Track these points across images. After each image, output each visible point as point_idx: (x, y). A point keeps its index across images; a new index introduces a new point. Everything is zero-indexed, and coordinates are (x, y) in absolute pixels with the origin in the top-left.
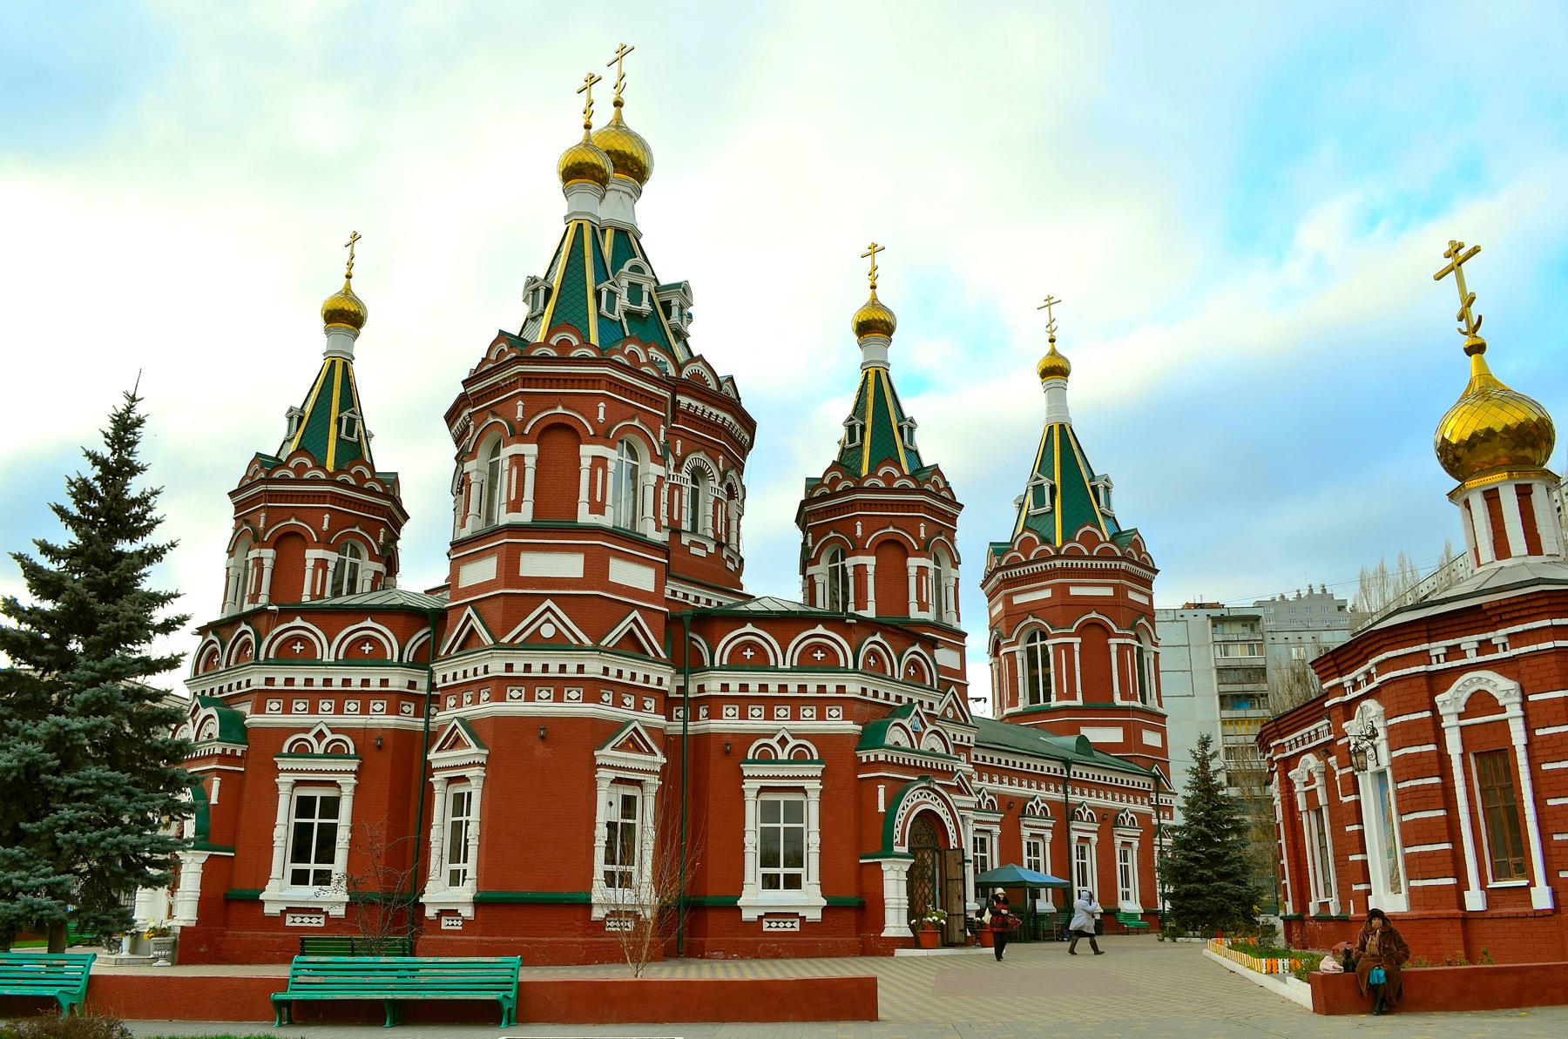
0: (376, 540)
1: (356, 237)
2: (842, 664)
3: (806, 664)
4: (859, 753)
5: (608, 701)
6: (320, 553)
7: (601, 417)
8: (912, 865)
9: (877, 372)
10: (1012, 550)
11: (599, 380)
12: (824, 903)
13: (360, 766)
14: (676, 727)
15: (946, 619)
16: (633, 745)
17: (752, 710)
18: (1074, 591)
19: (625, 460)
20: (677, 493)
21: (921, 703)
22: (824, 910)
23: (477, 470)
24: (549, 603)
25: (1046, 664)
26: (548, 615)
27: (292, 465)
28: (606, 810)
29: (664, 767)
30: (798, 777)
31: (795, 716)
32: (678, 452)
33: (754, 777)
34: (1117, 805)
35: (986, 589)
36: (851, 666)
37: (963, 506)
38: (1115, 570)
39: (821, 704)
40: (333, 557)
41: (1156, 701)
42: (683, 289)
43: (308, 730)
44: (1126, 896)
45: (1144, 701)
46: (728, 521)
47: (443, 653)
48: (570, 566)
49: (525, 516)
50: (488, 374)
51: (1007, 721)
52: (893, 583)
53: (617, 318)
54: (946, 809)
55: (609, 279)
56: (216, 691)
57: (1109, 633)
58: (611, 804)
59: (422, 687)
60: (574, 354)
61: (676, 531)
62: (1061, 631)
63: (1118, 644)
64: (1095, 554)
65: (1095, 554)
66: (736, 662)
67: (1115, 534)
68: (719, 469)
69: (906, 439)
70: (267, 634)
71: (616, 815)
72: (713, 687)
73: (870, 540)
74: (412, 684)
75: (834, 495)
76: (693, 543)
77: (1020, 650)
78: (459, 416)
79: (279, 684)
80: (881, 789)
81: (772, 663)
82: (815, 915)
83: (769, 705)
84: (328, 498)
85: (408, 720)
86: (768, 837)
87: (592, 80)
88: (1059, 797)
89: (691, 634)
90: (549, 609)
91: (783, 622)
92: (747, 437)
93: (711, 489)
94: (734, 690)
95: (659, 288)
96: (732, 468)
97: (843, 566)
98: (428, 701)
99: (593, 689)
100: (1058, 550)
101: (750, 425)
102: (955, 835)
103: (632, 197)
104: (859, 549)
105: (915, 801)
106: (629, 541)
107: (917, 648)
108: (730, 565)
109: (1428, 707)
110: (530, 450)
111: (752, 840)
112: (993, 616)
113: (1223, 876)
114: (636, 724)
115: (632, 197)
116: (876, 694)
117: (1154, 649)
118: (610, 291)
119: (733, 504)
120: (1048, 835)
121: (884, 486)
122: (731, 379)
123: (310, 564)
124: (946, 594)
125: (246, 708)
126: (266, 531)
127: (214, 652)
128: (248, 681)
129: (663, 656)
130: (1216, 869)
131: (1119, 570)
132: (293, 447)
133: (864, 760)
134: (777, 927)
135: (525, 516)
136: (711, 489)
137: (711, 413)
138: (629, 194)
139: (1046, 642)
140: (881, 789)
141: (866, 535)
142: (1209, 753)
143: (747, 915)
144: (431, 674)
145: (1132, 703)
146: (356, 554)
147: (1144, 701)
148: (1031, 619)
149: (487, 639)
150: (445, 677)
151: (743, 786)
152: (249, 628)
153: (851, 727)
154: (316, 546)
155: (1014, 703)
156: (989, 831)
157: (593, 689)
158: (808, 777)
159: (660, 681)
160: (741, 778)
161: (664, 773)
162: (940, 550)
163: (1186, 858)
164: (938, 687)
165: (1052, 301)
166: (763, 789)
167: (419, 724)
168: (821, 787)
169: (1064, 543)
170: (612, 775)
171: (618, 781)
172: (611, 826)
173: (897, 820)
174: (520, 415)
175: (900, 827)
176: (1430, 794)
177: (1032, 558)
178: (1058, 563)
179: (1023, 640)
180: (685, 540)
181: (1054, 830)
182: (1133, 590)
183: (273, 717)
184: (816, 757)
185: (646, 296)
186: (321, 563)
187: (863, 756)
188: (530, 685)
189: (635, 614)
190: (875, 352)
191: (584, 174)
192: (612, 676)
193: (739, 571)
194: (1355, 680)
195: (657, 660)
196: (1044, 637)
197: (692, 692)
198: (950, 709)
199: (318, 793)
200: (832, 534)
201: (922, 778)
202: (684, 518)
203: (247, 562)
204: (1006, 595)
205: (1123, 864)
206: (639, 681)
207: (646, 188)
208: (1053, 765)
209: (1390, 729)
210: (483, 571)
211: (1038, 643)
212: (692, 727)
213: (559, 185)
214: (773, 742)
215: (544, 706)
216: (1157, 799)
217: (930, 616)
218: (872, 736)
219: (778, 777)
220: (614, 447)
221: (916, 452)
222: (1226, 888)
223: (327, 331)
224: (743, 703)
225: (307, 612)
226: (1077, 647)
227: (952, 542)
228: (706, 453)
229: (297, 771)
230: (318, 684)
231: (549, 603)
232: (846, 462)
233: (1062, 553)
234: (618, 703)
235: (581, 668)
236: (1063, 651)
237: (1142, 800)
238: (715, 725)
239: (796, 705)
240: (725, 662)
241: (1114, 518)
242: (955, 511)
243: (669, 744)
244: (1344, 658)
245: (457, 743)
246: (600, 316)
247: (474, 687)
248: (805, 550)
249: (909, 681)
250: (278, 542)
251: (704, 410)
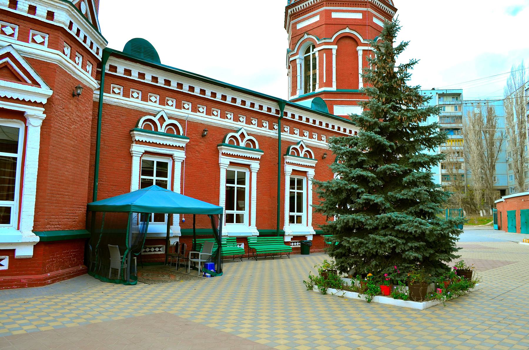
18: (334, 15)
57: (357, 43)
63: (363, 50)
88: (273, 134)
130: (389, 194)
142: (395, 45)
148: (306, 36)
156: (171, 156)
163: (351, 180)
168: (45, 116)
182: (377, 17)
208: (266, 105)
211: (311, 53)
226: (334, 52)
236: (325, 55)
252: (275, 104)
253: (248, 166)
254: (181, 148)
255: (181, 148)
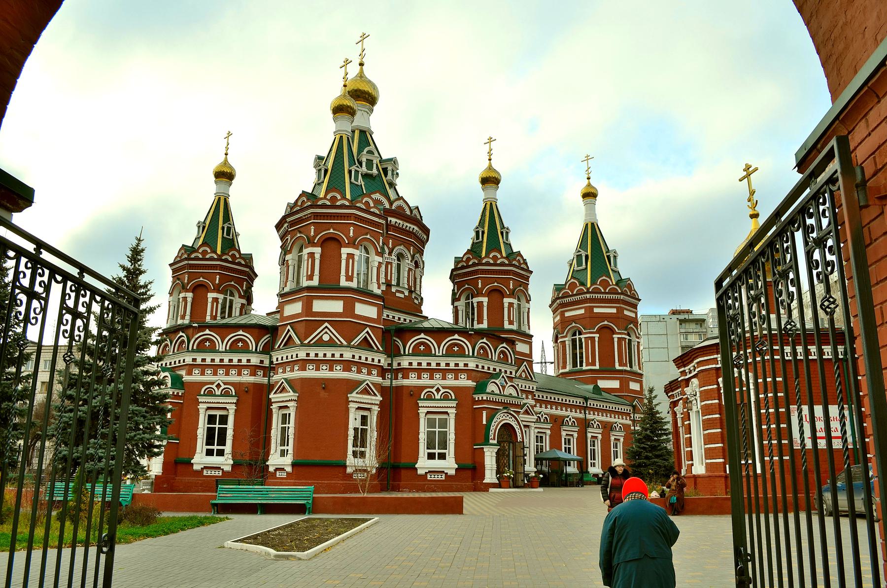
0: (242, 288)
1: (229, 134)
2: (467, 353)
3: (449, 353)
4: (474, 396)
5: (354, 371)
6: (215, 295)
7: (351, 234)
8: (499, 449)
9: (491, 203)
10: (565, 288)
11: (351, 216)
12: (456, 466)
13: (237, 400)
14: (387, 383)
15: (523, 329)
16: (366, 391)
17: (424, 375)
18: (596, 310)
19: (363, 254)
20: (389, 266)
21: (506, 372)
22: (457, 470)
23: (292, 259)
24: (326, 324)
25: (581, 347)
26: (326, 330)
27: (200, 251)
28: (354, 422)
29: (381, 401)
30: (445, 407)
31: (444, 378)
32: (390, 246)
33: (424, 407)
34: (613, 420)
35: (552, 308)
36: (471, 354)
37: (532, 272)
38: (618, 299)
39: (457, 372)
40: (221, 297)
41: (638, 367)
42: (393, 161)
43: (212, 383)
44: (593, 465)
45: (631, 367)
46: (415, 279)
47: (276, 347)
48: (337, 306)
49: (315, 282)
50: (297, 212)
51: (561, 376)
52: (496, 310)
53: (359, 184)
54: (516, 423)
55: (355, 164)
56: (168, 364)
57: (614, 332)
58: (356, 419)
59: (267, 363)
60: (338, 203)
61: (389, 285)
62: (589, 331)
64: (607, 291)
65: (607, 291)
66: (416, 352)
67: (619, 280)
68: (410, 254)
69: (504, 238)
70: (192, 338)
71: (358, 424)
72: (405, 364)
73: (485, 289)
74: (262, 362)
75: (468, 267)
76: (398, 291)
77: (568, 340)
78: (282, 226)
79: (199, 361)
80: (484, 413)
81: (433, 352)
82: (452, 472)
83: (432, 372)
84: (218, 268)
85: (260, 379)
86: (431, 436)
87: (347, 62)
88: (582, 416)
89: (394, 338)
90: (326, 327)
91: (440, 333)
92: (425, 237)
93: (407, 263)
94: (415, 365)
95: (382, 161)
96: (418, 253)
97: (472, 302)
98: (269, 370)
99: (347, 365)
100: (588, 289)
101: (427, 231)
102: (521, 435)
103: (368, 113)
104: (480, 294)
105: (501, 419)
106: (364, 294)
107: (504, 345)
108: (416, 301)
109: (716, 383)
110: (317, 251)
111: (423, 437)
112: (555, 322)
113: (657, 456)
114: (368, 382)
115: (368, 113)
116: (483, 367)
117: (637, 340)
118: (356, 170)
119: (418, 270)
120: (576, 435)
121: (493, 262)
122: (417, 208)
123: (210, 300)
124: (523, 316)
125: (183, 373)
126: (188, 284)
127: (167, 345)
128: (184, 360)
129: (381, 349)
130: (654, 453)
131: (619, 300)
132: (200, 242)
133: (477, 399)
134: (434, 477)
135: (315, 282)
136: (407, 263)
137: (407, 226)
138: (367, 112)
139: (581, 336)
140: (484, 413)
141: (483, 287)
142: (653, 396)
143: (420, 472)
144: (271, 357)
145: (625, 368)
146: (232, 295)
147: (631, 367)
148: (574, 324)
149: (298, 342)
150: (277, 359)
151: (419, 411)
152: (184, 335)
153: (471, 383)
154: (213, 291)
155: (564, 367)
156: (545, 433)
157: (347, 365)
158: (449, 407)
159: (379, 361)
160: (418, 407)
161: (381, 405)
162: (520, 294)
163: (639, 447)
164: (515, 364)
165: (589, 158)
166: (428, 413)
167: (265, 380)
169: (591, 285)
170: (357, 405)
171: (359, 408)
172: (356, 429)
173: (492, 428)
174: (312, 233)
175: (493, 431)
176: (715, 422)
177: (575, 293)
178: (588, 296)
179: (569, 335)
180: (394, 290)
181: (578, 432)
183: (196, 377)
184: (453, 398)
185: (375, 166)
186: (216, 300)
187: (476, 397)
188: (318, 363)
189: (368, 329)
190: (490, 193)
191: (343, 110)
192: (356, 359)
193: (421, 304)
194: (690, 369)
195: (378, 351)
196: (580, 334)
197: (395, 366)
198: (523, 373)
199: (218, 413)
200: (467, 286)
201: (504, 408)
202: (393, 279)
203: (179, 299)
204: (561, 312)
205: (615, 449)
206: (369, 361)
207: (375, 108)
208: (579, 400)
209: (701, 392)
210: (294, 309)
211: (577, 337)
212: (395, 383)
213: (331, 116)
214: (433, 390)
215: (324, 373)
216: (634, 417)
217: (514, 327)
218: (481, 388)
219: (435, 407)
220: (357, 249)
221: (510, 244)
222: (658, 462)
223: (216, 182)
224: (419, 371)
225: (211, 327)
226: (597, 339)
227: (527, 291)
228: (405, 246)
229: (208, 402)
230: (217, 362)
231: (326, 324)
232: (475, 250)
233: (590, 290)
234: (359, 371)
235: (341, 355)
236: (590, 341)
237: (622, 417)
238: (406, 382)
239: (444, 372)
240: (411, 352)
241: (618, 272)
242: (528, 275)
243: (383, 390)
244: (686, 359)
245: (283, 390)
246: (351, 183)
247: (291, 364)
248: (454, 294)
249: (500, 361)
250: (194, 290)
251: (403, 225)
252: (582, 399)
253: (572, 435)
254: (548, 429)
255: (548, 429)
